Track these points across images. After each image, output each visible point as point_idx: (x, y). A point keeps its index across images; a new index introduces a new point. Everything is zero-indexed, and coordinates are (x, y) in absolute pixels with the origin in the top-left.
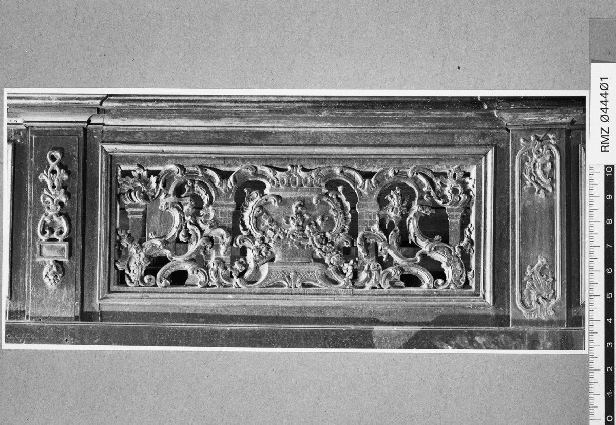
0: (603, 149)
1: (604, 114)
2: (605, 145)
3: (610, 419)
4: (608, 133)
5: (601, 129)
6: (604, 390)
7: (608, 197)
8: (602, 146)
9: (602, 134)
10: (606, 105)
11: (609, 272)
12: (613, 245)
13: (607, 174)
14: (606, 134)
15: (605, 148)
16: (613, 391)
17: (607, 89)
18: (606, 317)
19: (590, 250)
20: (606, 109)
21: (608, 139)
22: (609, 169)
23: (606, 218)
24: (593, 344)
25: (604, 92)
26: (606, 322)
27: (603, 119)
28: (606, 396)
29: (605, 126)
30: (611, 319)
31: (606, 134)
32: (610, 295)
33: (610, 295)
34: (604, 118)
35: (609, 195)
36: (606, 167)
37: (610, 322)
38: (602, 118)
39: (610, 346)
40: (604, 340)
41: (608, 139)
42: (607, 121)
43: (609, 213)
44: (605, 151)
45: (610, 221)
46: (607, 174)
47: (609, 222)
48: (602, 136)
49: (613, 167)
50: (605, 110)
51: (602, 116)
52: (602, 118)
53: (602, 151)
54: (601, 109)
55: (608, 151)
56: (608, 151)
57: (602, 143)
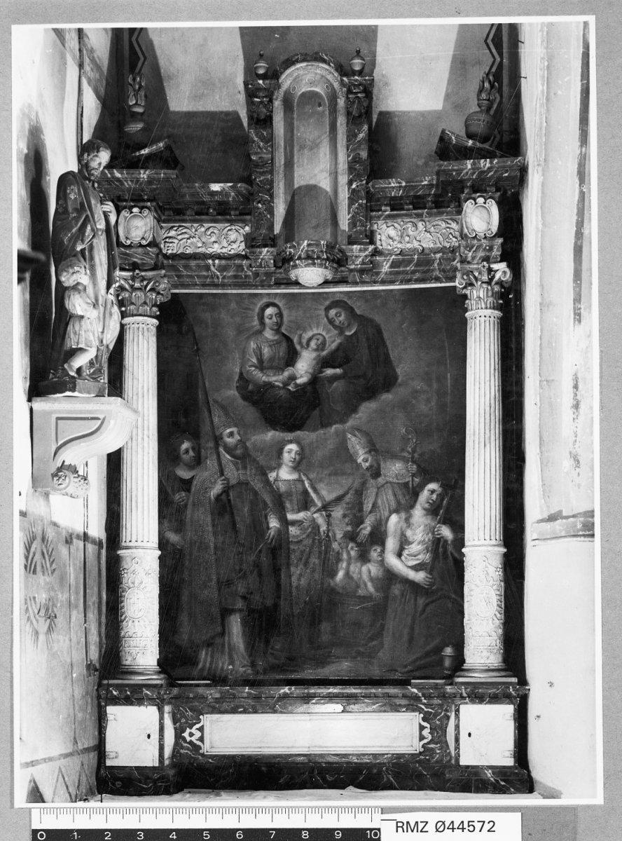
0: (400, 824)
1: (446, 827)
2: (405, 827)
3: (42, 836)
5: (427, 822)
6: (80, 828)
7: (338, 833)
9: (419, 823)
11: (237, 835)
14: (420, 830)
15: (401, 827)
20: (453, 829)
21: (412, 831)
22: (376, 834)
24: (207, 813)
26: (171, 831)
27: (440, 824)
29: (431, 827)
30: (175, 837)
31: (420, 830)
33: (206, 836)
34: (440, 827)
35: (340, 835)
36: (379, 830)
37: (171, 837)
39: (138, 836)
41: (412, 831)
42: (437, 830)
44: (397, 827)
45: (306, 836)
48: (417, 822)
50: (451, 827)
51: (444, 823)
54: (452, 822)
55: (397, 831)
56: (397, 831)
57: (408, 823)
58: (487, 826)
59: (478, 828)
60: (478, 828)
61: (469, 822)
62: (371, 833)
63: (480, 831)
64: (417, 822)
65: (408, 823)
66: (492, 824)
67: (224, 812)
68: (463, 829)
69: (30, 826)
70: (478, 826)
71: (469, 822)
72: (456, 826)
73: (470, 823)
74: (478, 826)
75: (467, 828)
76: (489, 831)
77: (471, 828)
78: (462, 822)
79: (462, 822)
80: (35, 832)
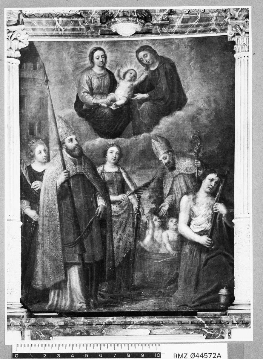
0: (175, 355)
2: (177, 356)
4: (184, 358)
5: (187, 354)
7: (143, 355)
8: (177, 354)
9: (184, 355)
10: (200, 357)
11: (100, 355)
12: (115, 358)
13: (156, 354)
14: (184, 357)
16: (32, 358)
18: (75, 354)
19: (112, 345)
20: (198, 357)
21: (181, 358)
22: (159, 355)
27: (192, 355)
28: (29, 354)
29: (188, 356)
30: (73, 356)
31: (184, 357)
32: (87, 356)
33: (87, 356)
35: (144, 355)
38: (193, 354)
39: (58, 356)
41: (181, 358)
42: (191, 357)
43: (133, 355)
44: (174, 356)
45: (129, 356)
46: (156, 354)
47: (129, 355)
48: (183, 354)
49: (160, 357)
50: (197, 356)
51: (194, 354)
52: (193, 354)
53: (174, 354)
54: (198, 354)
57: (179, 354)
58: (213, 356)
59: (209, 356)
60: (209, 356)
61: (205, 354)
62: (156, 355)
63: (210, 358)
65: (179, 354)
66: (215, 354)
67: (94, 346)
68: (202, 357)
70: (209, 355)
71: (205, 354)
72: (199, 356)
73: (205, 354)
74: (209, 355)
75: (204, 356)
76: (213, 357)
77: (206, 356)
78: (202, 354)
79: (202, 354)
80: (14, 354)
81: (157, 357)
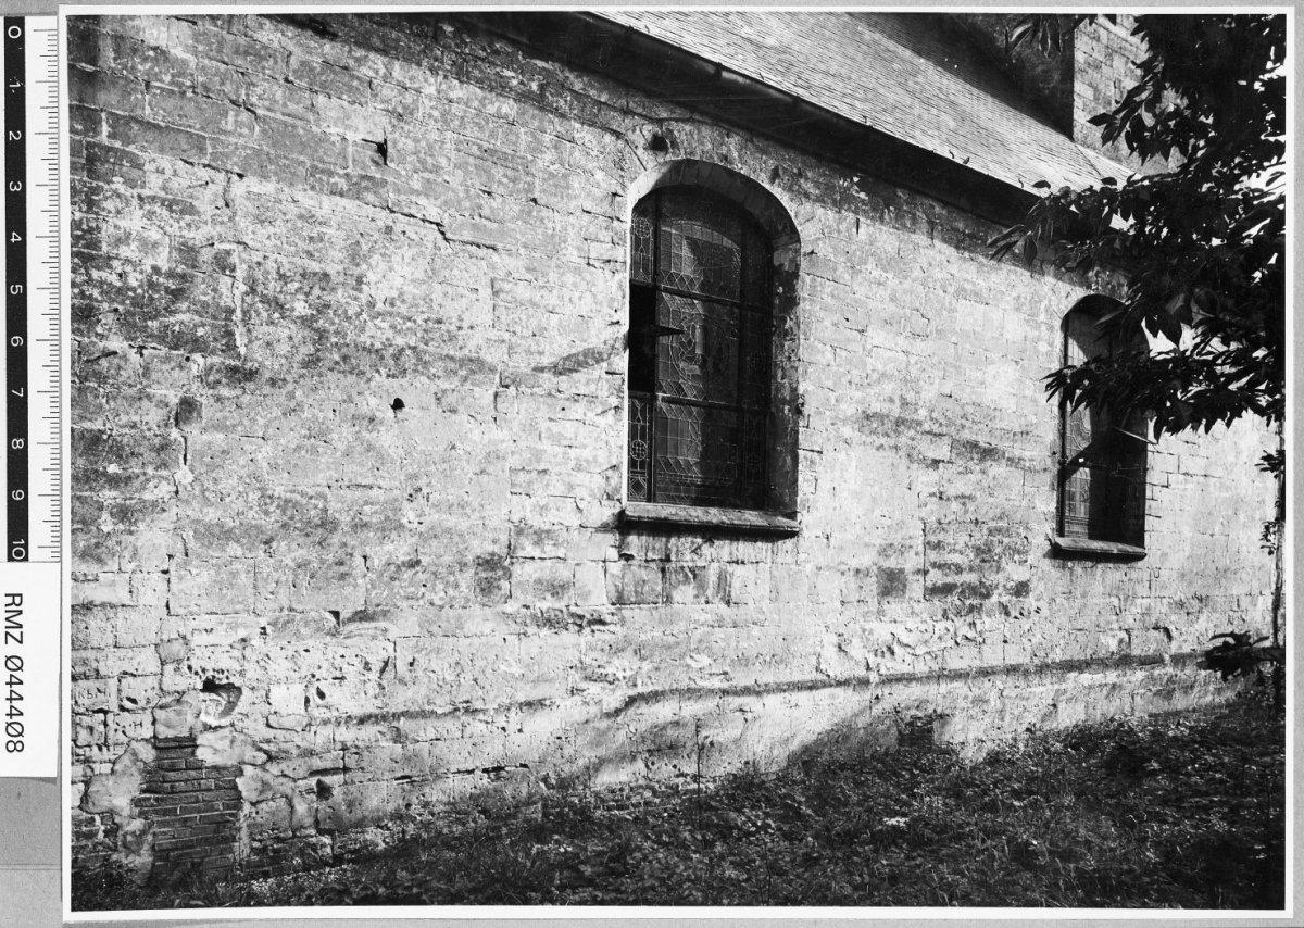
0: (17, 600)
1: (14, 673)
2: (13, 608)
3: (14, 32)
5: (21, 642)
7: (20, 495)
9: (19, 630)
12: (9, 394)
14: (9, 631)
15: (14, 603)
16: (7, 90)
17: (9, 724)
18: (23, 244)
20: (10, 683)
21: (7, 619)
22: (19, 553)
23: (25, 451)
25: (15, 719)
26: (23, 234)
28: (22, 79)
29: (13, 648)
30: (13, 240)
31: (9, 631)
32: (14, 289)
33: (14, 289)
36: (26, 559)
38: (19, 664)
39: (16, 184)
40: (28, 196)
41: (7, 619)
42: (8, 659)
44: (14, 596)
48: (21, 626)
49: (10, 559)
50: (14, 680)
51: (20, 669)
52: (19, 664)
53: (21, 595)
54: (21, 683)
57: (20, 612)
64: (21, 626)
69: (30, 14)
72: (15, 687)
80: (20, 22)
81: (10, 547)
